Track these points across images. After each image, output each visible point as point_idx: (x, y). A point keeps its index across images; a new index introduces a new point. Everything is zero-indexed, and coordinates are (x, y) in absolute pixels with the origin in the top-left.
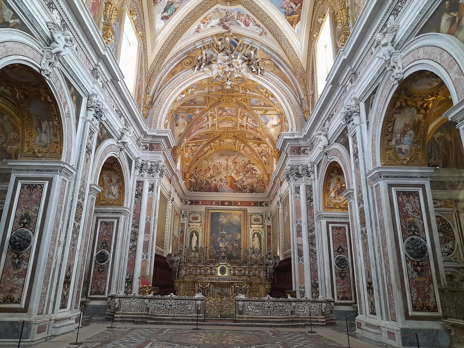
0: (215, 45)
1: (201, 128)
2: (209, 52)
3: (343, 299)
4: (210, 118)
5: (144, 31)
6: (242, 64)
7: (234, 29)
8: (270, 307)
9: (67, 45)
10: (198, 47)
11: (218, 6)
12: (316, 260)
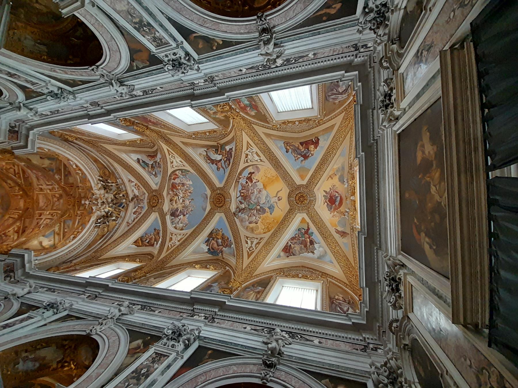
0: (119, 192)
1: (38, 179)
2: (114, 188)
4: (50, 187)
5: (129, 146)
6: (104, 211)
7: (131, 205)
9: (118, 93)
10: (118, 181)
11: (147, 194)
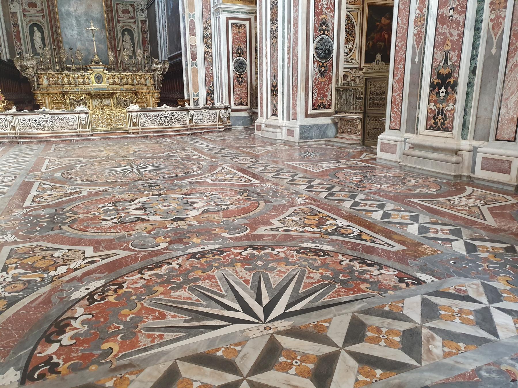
3: (239, 105)
8: (167, 116)
12: (212, 63)
